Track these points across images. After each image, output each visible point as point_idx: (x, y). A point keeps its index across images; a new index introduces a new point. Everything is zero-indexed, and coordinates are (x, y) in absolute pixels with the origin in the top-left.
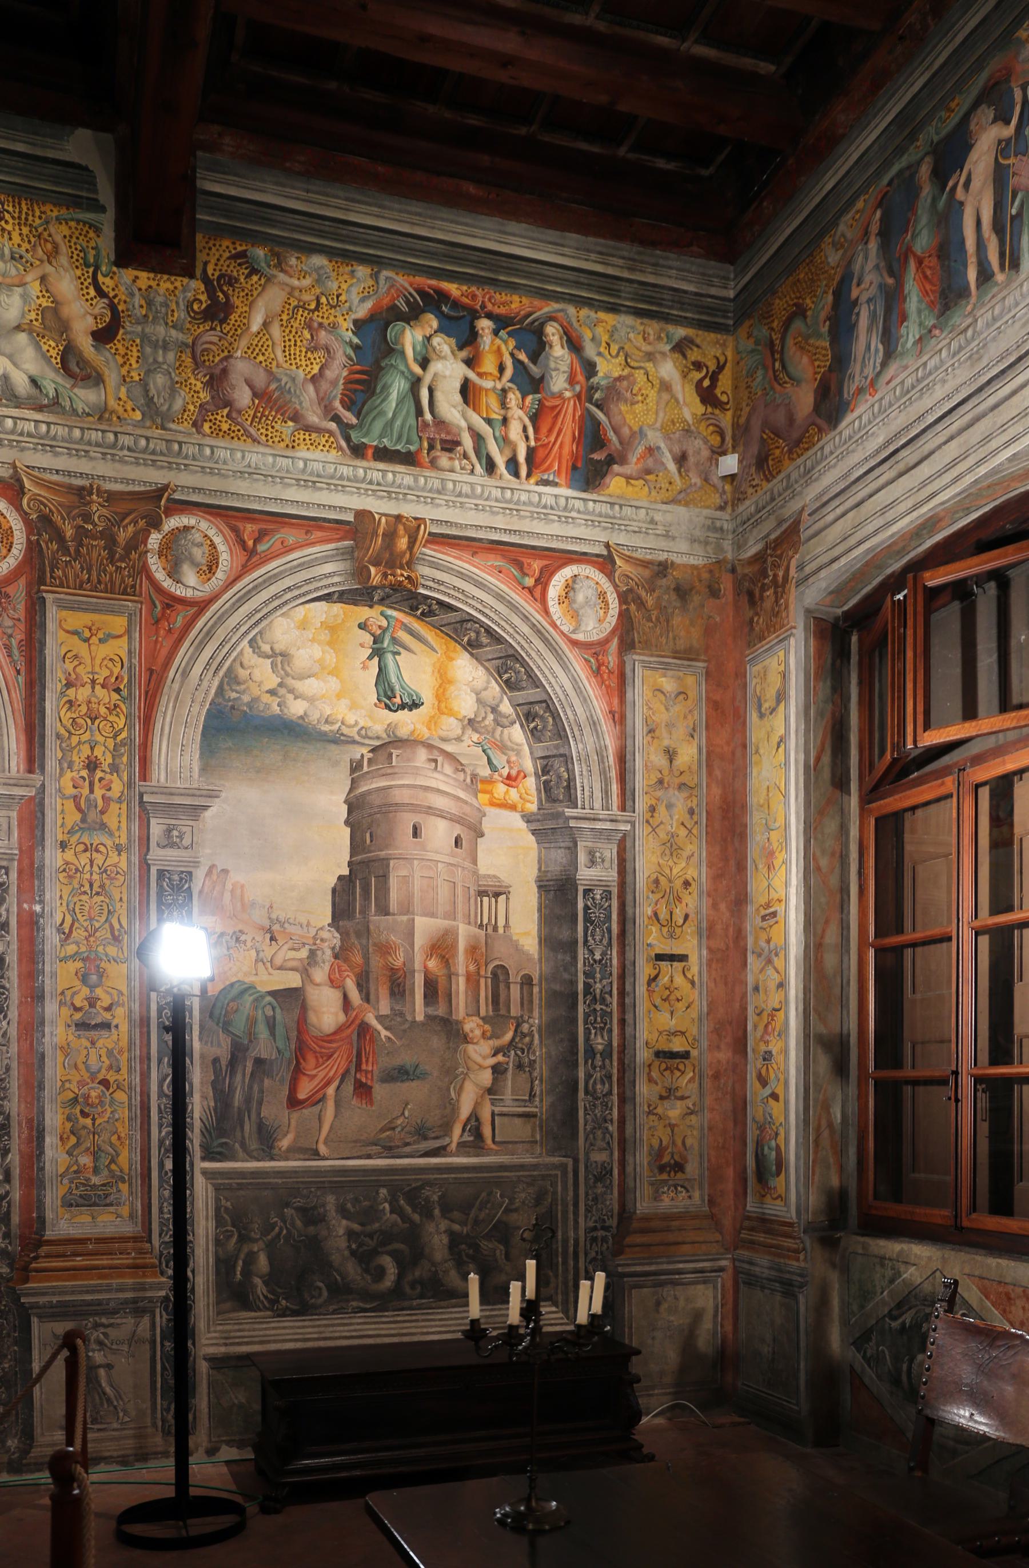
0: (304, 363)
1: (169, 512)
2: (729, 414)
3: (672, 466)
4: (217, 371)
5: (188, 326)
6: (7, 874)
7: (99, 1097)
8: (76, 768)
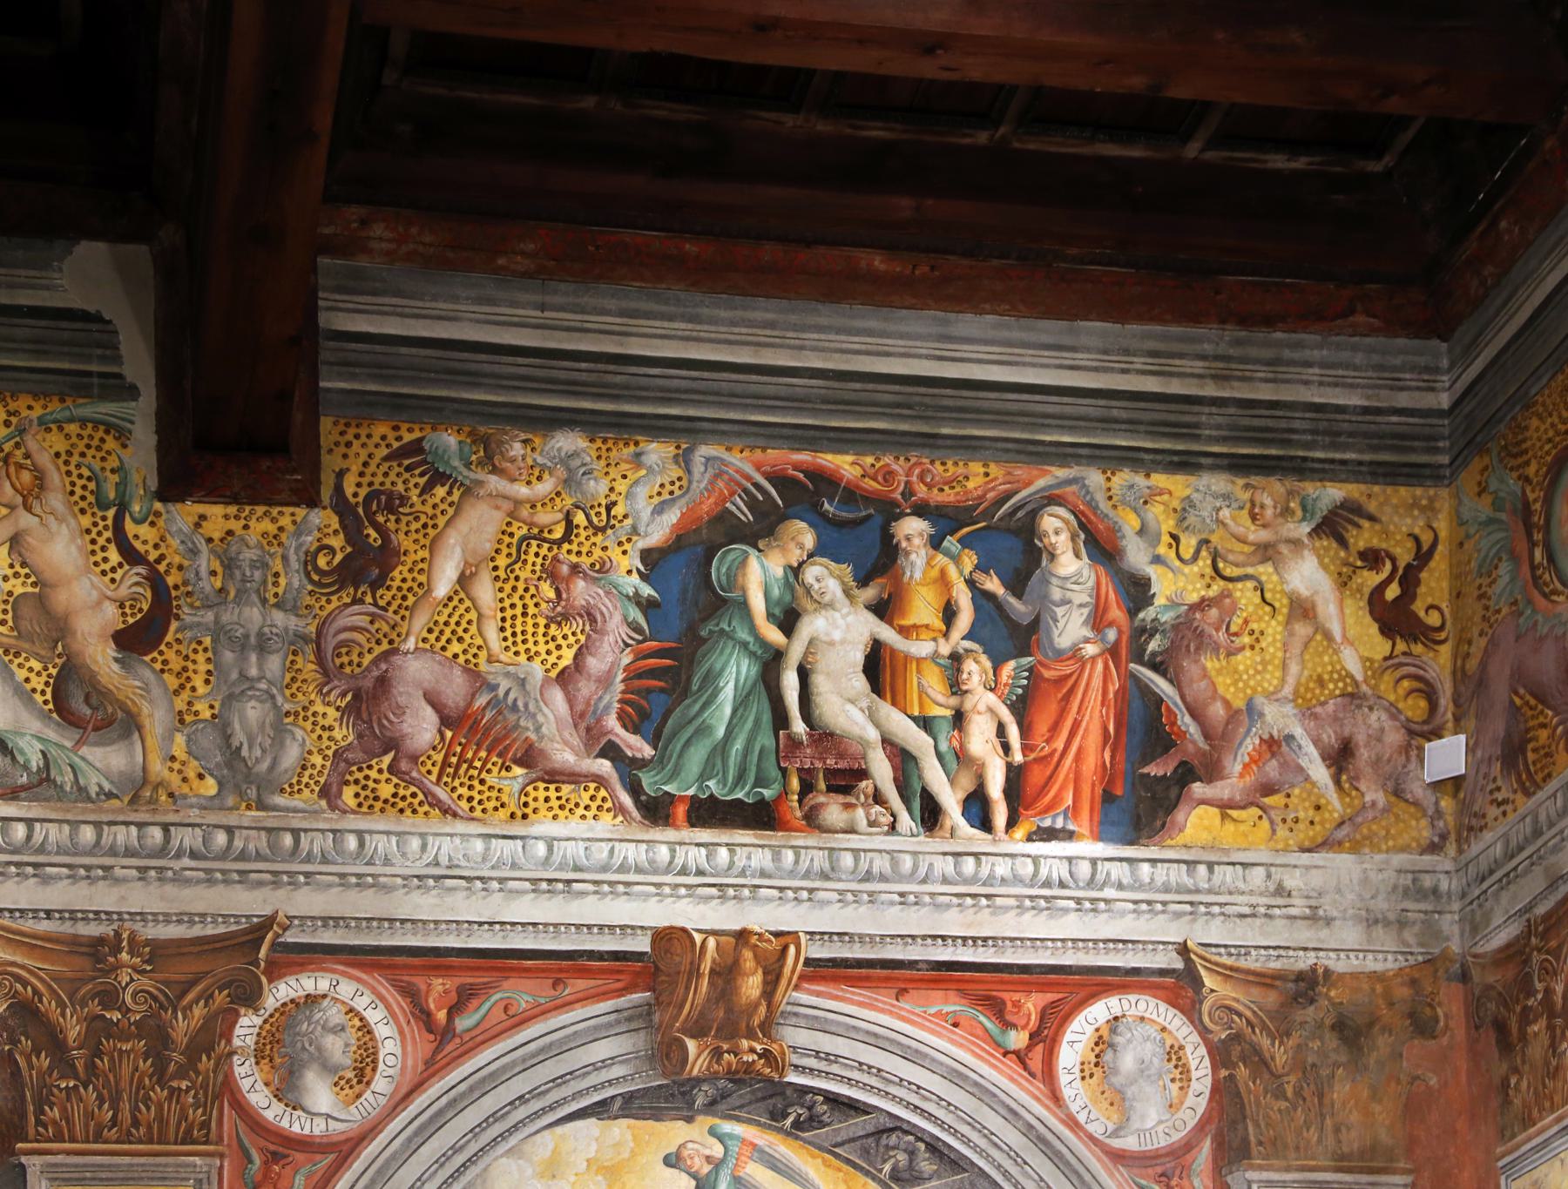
0: (542, 648)
1: (276, 971)
2: (1445, 650)
3: (1320, 773)
4: (368, 683)
5: (308, 600)
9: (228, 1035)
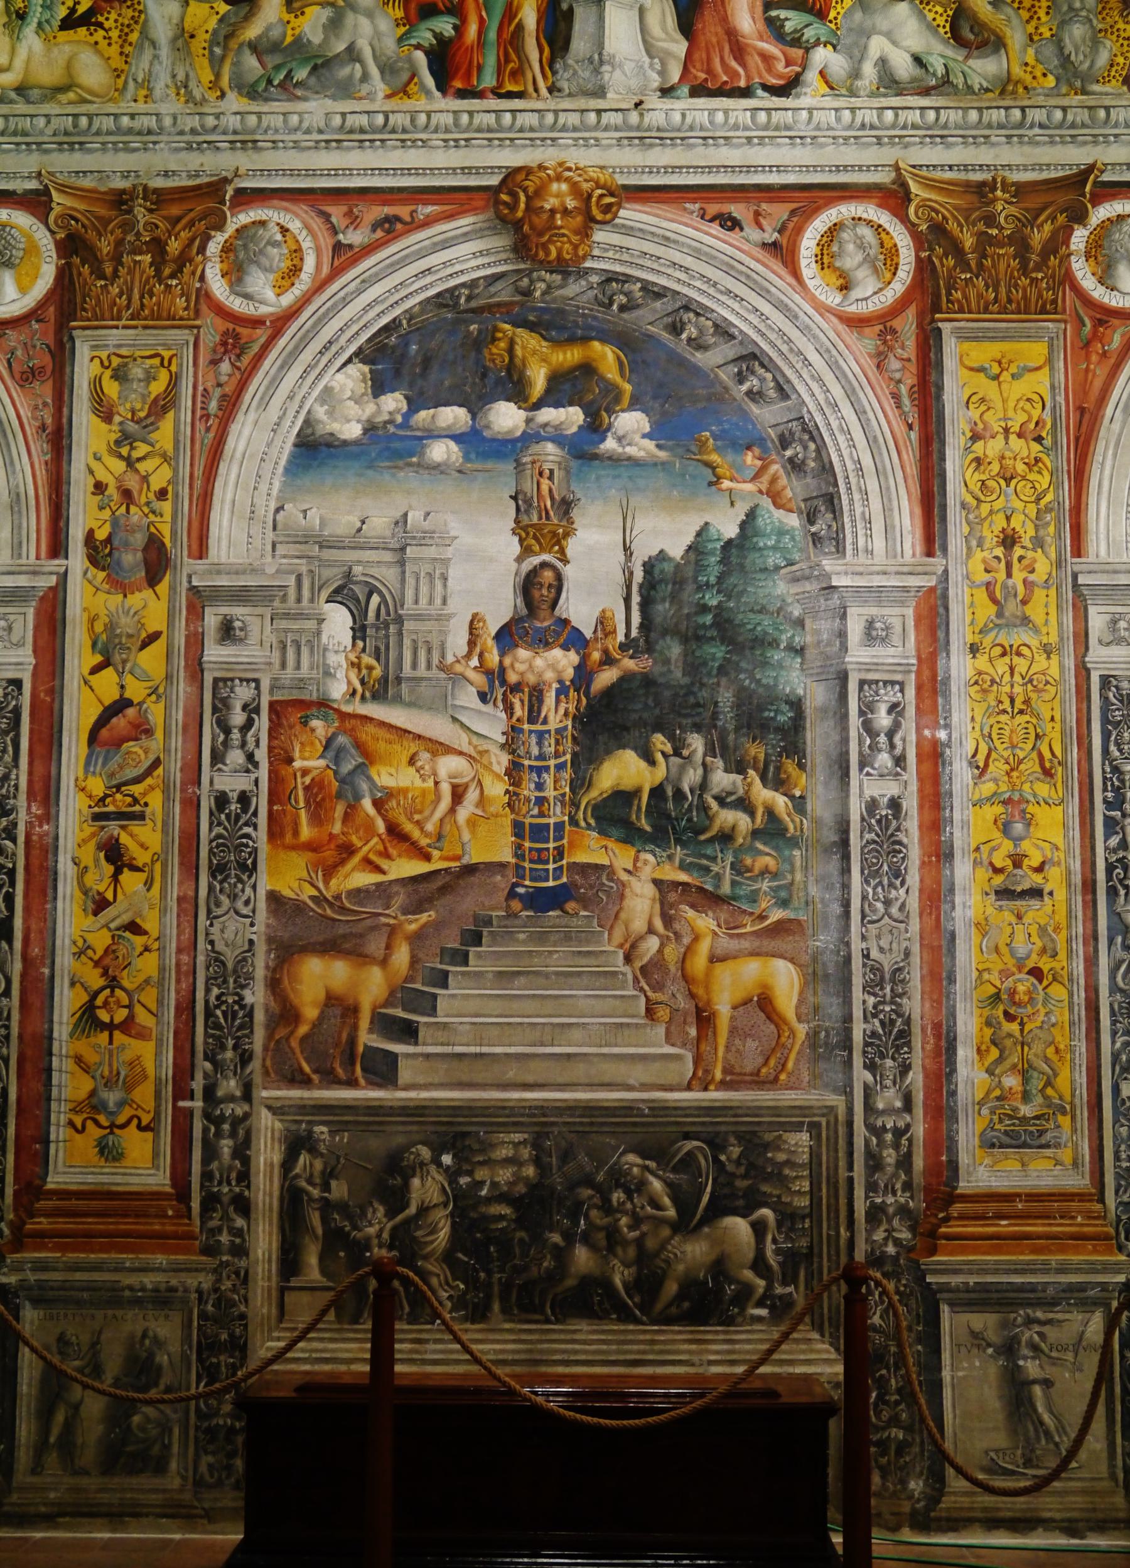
1: (1097, 199)
6: (902, 691)
7: (1029, 992)
8: (987, 545)
9: (1067, 242)
